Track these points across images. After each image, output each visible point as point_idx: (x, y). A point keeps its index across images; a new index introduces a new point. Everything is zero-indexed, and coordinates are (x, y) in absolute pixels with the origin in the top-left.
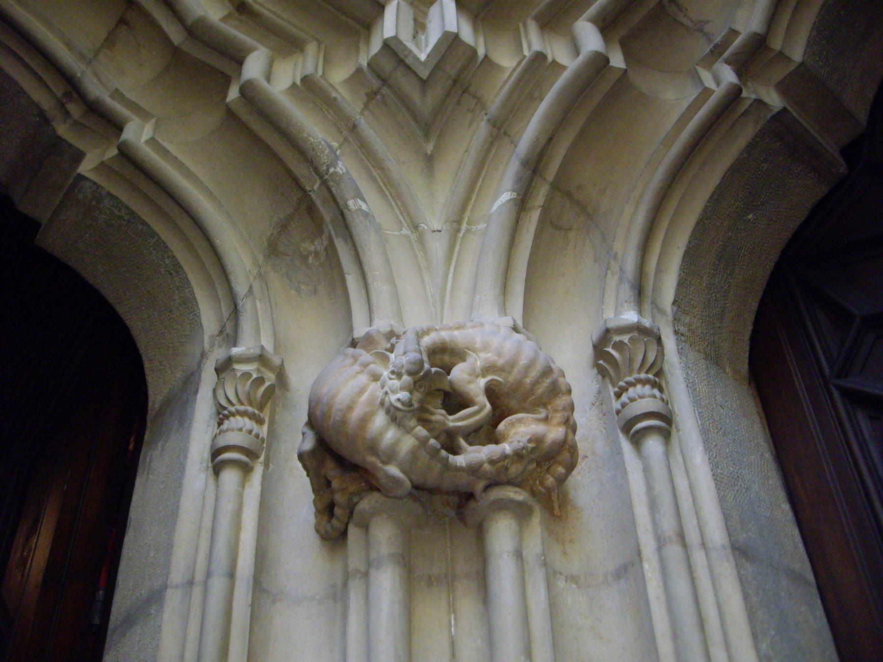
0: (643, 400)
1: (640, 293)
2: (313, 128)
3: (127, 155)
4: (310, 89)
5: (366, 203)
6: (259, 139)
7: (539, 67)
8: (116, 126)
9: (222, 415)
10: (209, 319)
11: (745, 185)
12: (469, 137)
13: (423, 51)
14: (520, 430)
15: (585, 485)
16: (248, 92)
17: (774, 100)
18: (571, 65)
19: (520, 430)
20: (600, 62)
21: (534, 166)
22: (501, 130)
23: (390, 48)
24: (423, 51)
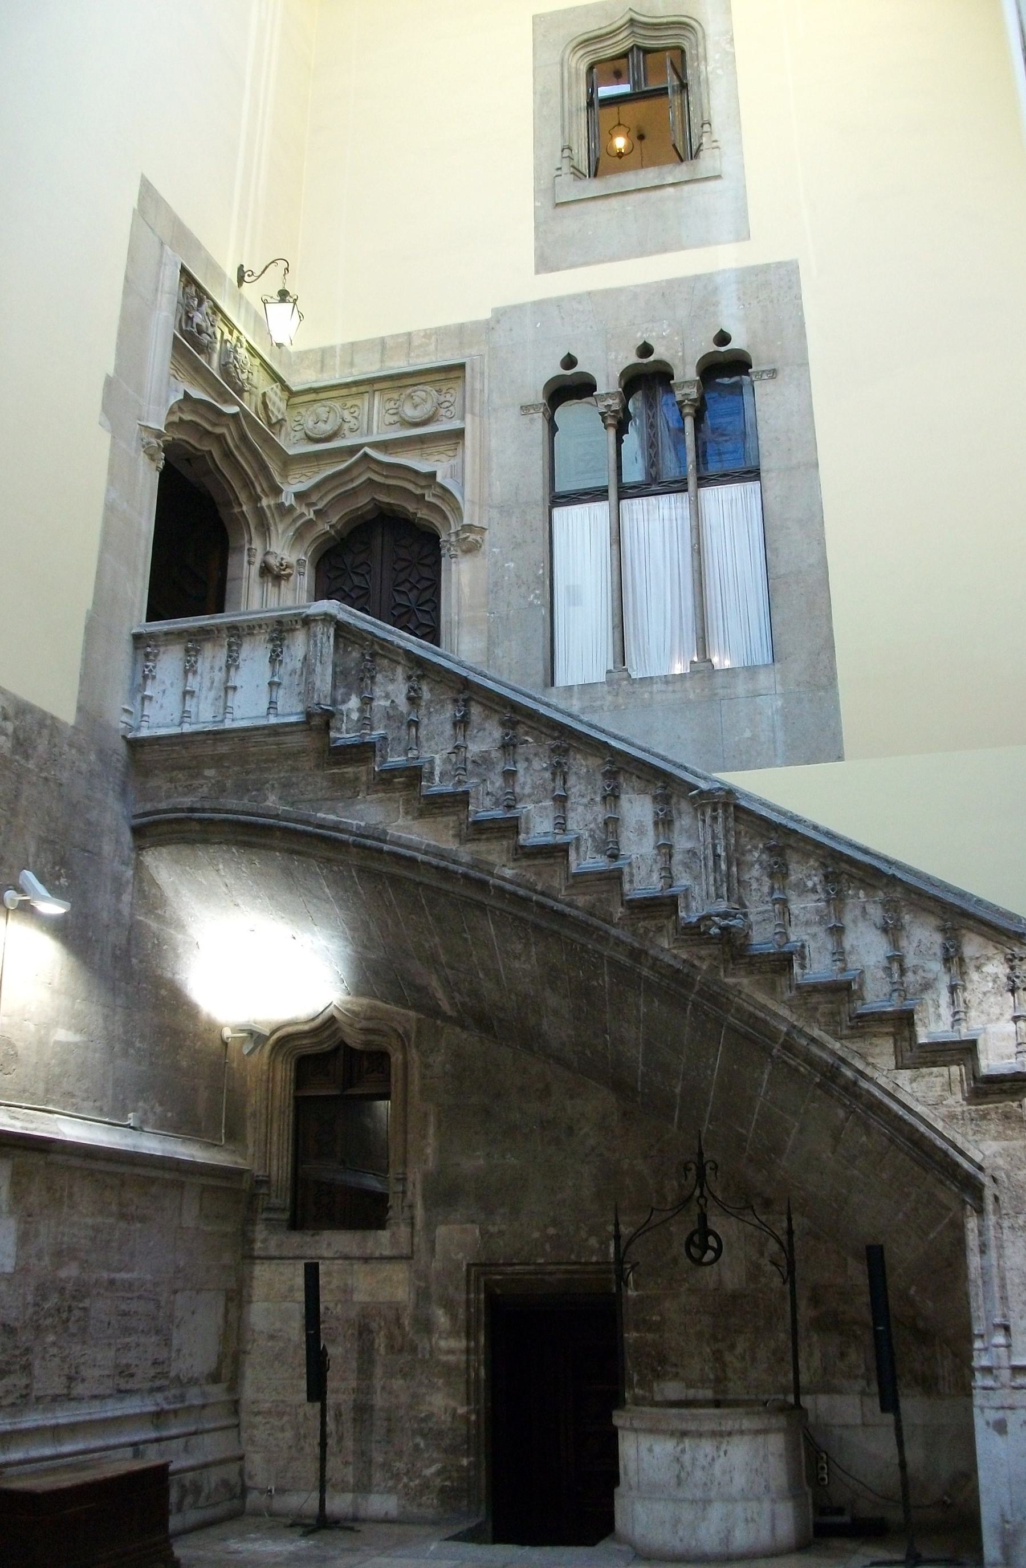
0: (302, 570)
1: (306, 554)
2: (269, 514)
3: (243, 512)
4: (269, 506)
5: (272, 528)
6: (260, 513)
7: (303, 515)
8: (241, 505)
9: (249, 556)
10: (246, 538)
11: (324, 542)
12: (288, 520)
13: (287, 504)
14: (288, 571)
15: (292, 578)
16: (262, 508)
17: (333, 533)
18: (307, 518)
19: (288, 571)
20: (311, 520)
21: (298, 529)
22: (294, 521)
23: (283, 503)
24: (287, 504)
